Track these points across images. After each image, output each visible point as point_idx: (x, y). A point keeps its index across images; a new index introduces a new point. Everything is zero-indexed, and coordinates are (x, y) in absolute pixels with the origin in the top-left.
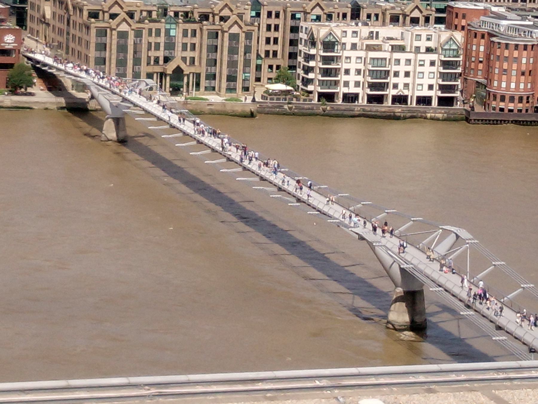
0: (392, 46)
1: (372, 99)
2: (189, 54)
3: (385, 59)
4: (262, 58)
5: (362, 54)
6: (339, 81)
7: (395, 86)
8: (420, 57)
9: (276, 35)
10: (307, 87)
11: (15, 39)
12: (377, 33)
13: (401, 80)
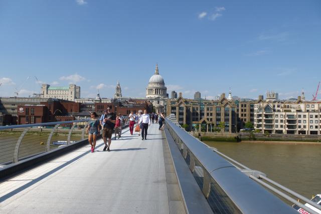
0: (297, 110)
1: (288, 132)
2: (210, 117)
5: (284, 113)
7: (300, 127)
8: (310, 114)
12: (288, 106)
13: (302, 124)
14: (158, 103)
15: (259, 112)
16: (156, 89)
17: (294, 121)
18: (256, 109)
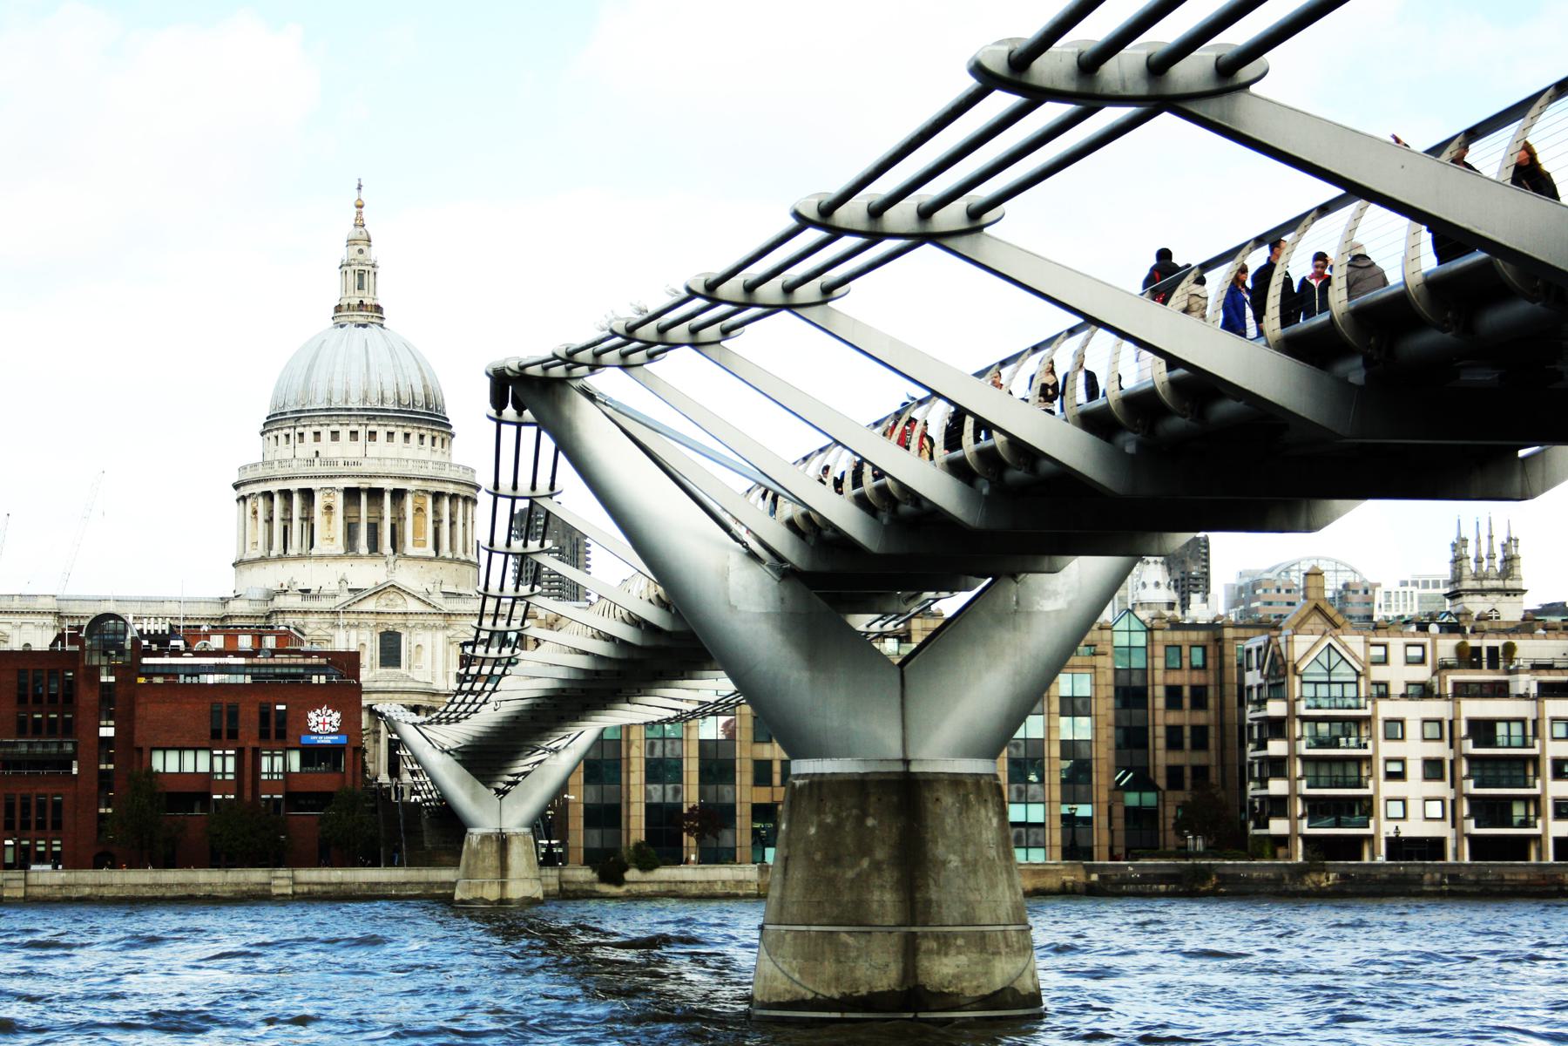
0: (1541, 685)
3: (1523, 721)
4: (1155, 788)
6: (1370, 798)
9: (1201, 718)
10: (1267, 827)
11: (343, 719)
14: (390, 652)
15: (1261, 703)
16: (351, 495)
17: (1521, 768)
18: (1253, 678)
